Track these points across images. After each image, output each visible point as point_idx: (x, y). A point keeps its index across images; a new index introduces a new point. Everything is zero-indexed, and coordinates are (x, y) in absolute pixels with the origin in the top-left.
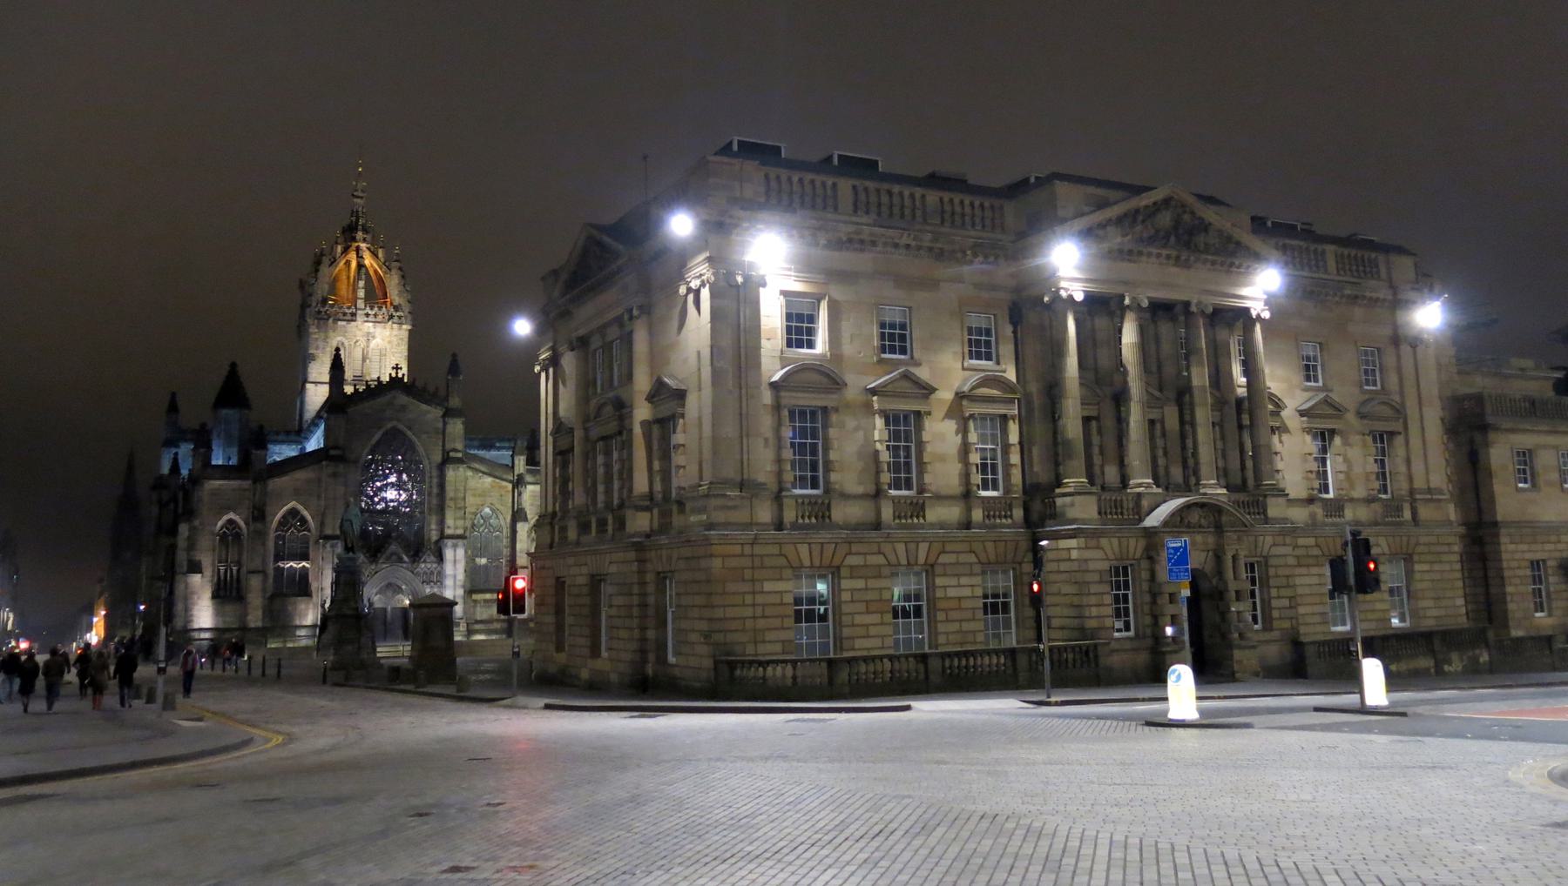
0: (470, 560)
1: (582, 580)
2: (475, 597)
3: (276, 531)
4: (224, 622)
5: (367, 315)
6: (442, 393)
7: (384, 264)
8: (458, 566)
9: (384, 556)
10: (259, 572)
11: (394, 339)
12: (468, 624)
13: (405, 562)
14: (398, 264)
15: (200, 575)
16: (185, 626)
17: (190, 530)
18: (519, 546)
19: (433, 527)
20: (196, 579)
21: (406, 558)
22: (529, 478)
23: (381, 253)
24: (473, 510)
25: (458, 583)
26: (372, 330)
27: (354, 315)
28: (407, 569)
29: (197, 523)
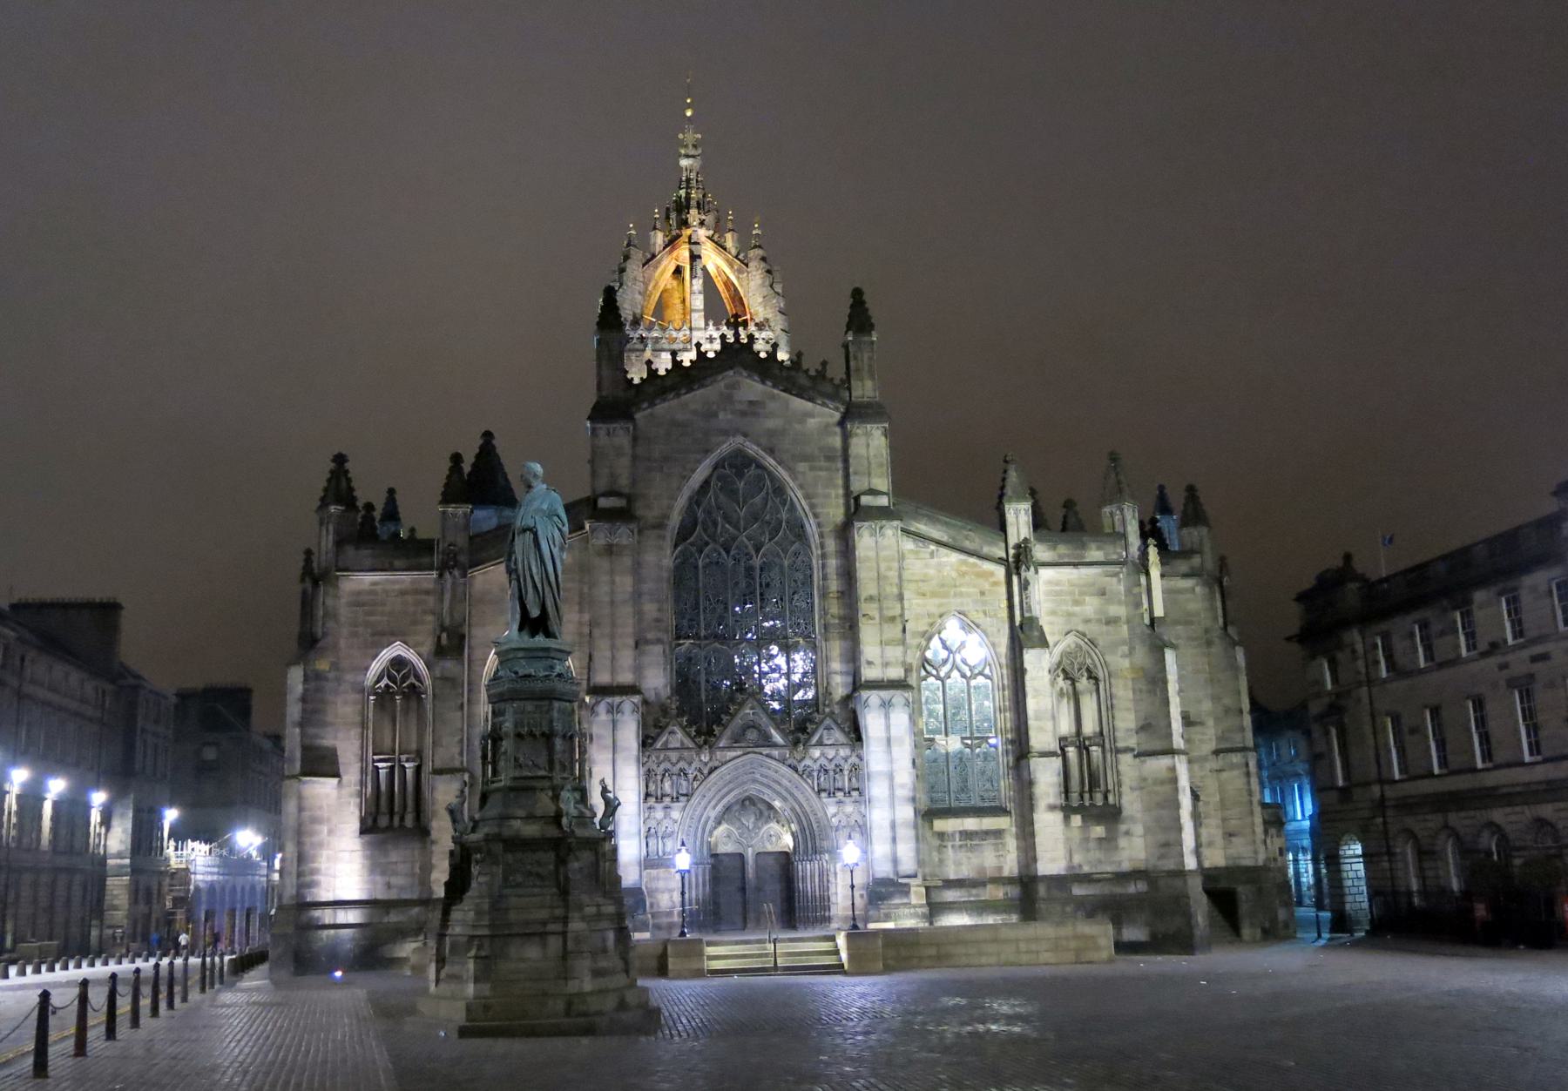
0: (922, 742)
2: (940, 825)
4: (389, 886)
6: (836, 372)
8: (895, 749)
9: (728, 732)
10: (452, 771)
12: (927, 888)
13: (775, 746)
14: (759, 252)
15: (335, 781)
16: (299, 895)
17: (306, 679)
18: (1032, 704)
19: (836, 665)
21: (777, 738)
22: (1040, 552)
23: (730, 241)
24: (922, 627)
25: (903, 792)
28: (783, 761)
29: (323, 665)
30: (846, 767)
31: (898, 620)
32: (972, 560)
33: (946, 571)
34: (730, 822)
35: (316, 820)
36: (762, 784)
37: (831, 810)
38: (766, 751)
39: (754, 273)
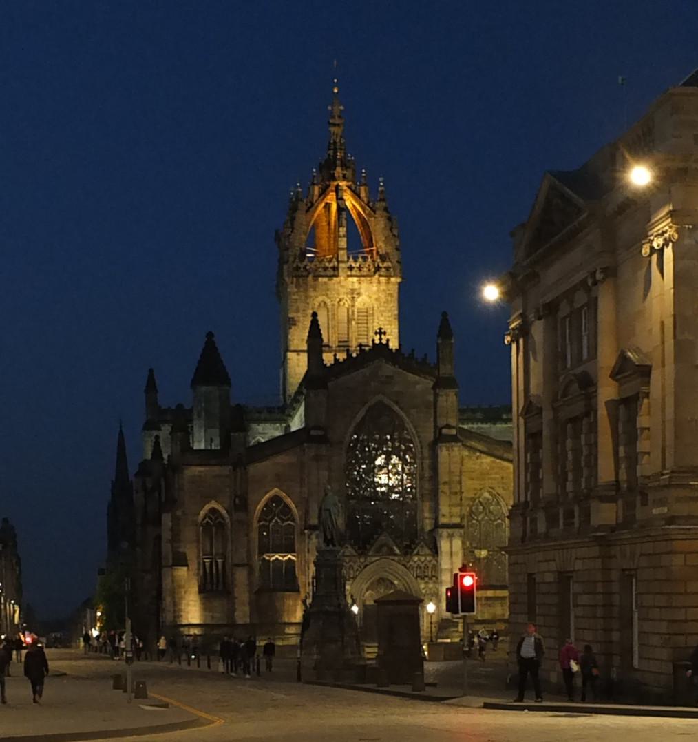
1: (550, 578)
3: (259, 521)
4: (213, 617)
5: (351, 268)
6: (432, 359)
7: (368, 204)
8: (454, 557)
9: (373, 549)
10: (243, 565)
11: (382, 296)
13: (396, 555)
14: (384, 204)
15: (185, 568)
16: (174, 621)
19: (427, 515)
20: (182, 572)
21: (398, 551)
24: (471, 495)
26: (356, 286)
27: (335, 269)
29: (179, 513)
30: (430, 566)
31: (459, 494)
32: (498, 461)
33: (485, 466)
34: (372, 590)
35: (180, 587)
36: (389, 573)
37: (422, 586)
38: (391, 557)
39: (380, 219)
